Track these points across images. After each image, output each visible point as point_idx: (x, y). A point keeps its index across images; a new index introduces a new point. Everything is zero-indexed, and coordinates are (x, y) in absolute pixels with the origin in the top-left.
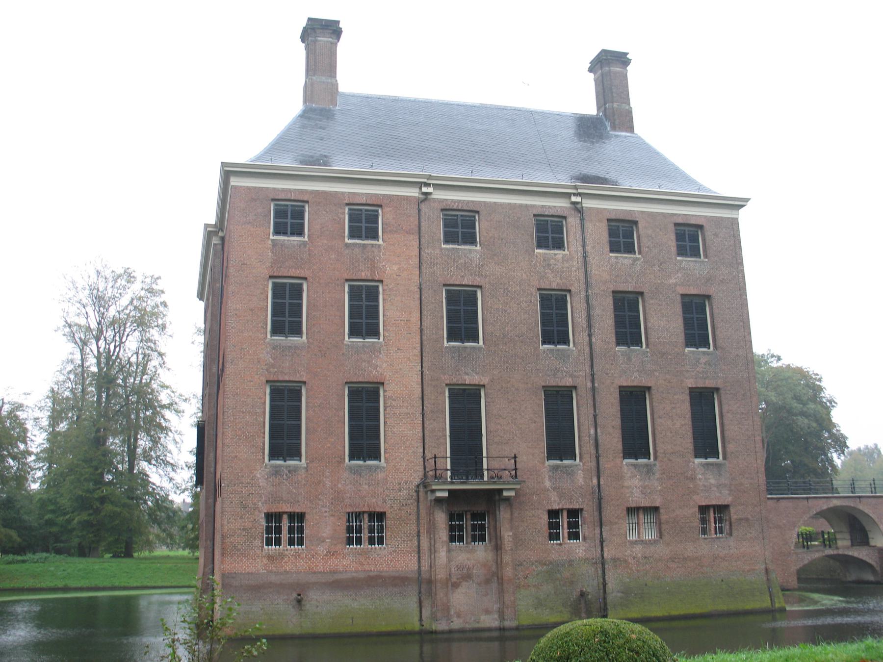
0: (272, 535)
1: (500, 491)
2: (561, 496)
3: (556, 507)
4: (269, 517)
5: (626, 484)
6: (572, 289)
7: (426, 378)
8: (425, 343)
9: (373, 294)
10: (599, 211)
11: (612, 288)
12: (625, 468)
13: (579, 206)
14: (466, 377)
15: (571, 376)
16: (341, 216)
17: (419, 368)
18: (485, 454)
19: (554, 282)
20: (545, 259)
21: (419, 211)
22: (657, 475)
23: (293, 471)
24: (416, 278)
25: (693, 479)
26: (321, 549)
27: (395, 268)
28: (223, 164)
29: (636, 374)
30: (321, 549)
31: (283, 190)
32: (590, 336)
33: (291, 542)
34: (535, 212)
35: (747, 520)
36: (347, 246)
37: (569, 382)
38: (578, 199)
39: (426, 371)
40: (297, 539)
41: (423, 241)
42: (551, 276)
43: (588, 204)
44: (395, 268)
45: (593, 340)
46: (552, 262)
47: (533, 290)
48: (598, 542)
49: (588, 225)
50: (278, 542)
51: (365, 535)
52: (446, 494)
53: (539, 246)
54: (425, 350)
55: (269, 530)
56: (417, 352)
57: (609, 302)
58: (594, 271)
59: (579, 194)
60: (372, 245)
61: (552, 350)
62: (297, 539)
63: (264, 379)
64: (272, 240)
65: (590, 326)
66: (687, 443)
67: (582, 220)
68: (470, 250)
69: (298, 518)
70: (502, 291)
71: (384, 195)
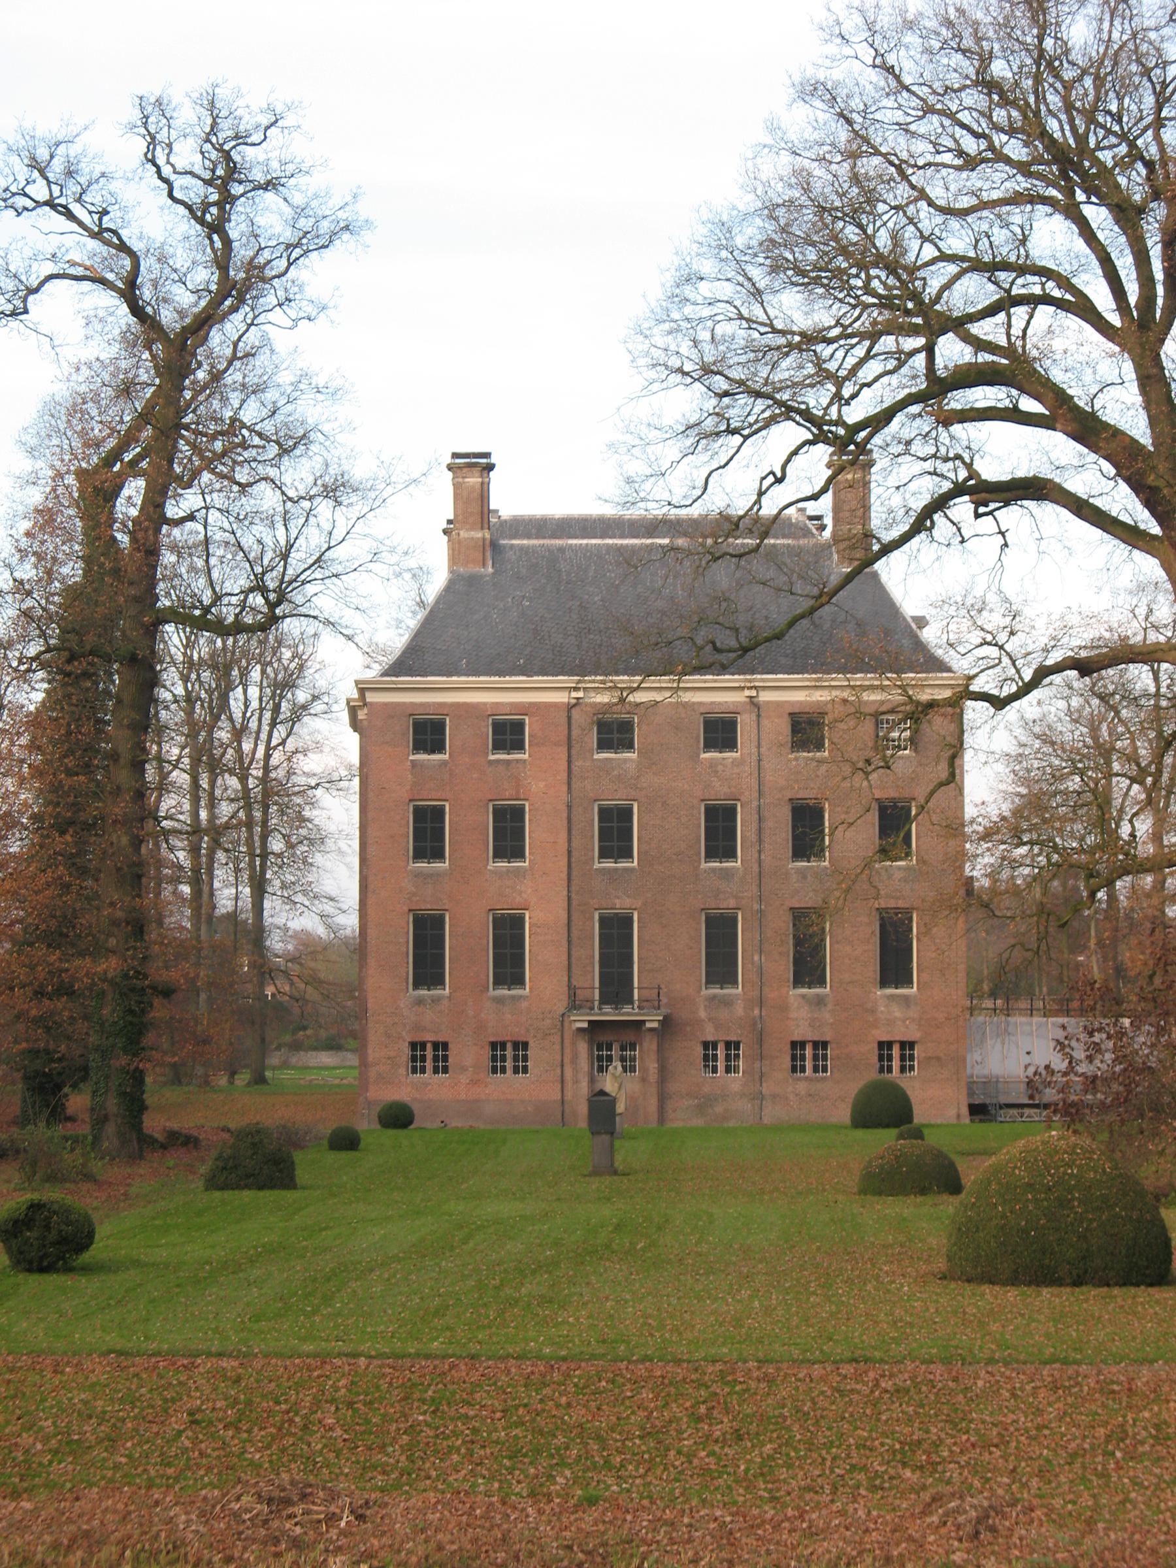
0: (417, 1063)
1: (644, 1022)
2: (717, 1028)
3: (710, 1038)
4: (413, 1046)
5: (791, 1016)
6: (742, 798)
7: (574, 903)
8: (573, 865)
9: (517, 814)
10: (779, 705)
11: (789, 795)
12: (792, 1000)
13: (755, 700)
14: (617, 901)
15: (736, 897)
16: (484, 730)
17: (565, 893)
18: (636, 984)
19: (719, 791)
20: (712, 764)
21: (569, 718)
22: (830, 1007)
23: (436, 1000)
24: (564, 796)
25: (873, 1011)
26: (464, 1079)
27: (541, 785)
28: (357, 682)
29: (811, 894)
30: (464, 1079)
31: (422, 705)
32: (760, 852)
33: (436, 1070)
34: (702, 710)
35: (938, 1059)
36: (491, 762)
37: (732, 903)
38: (753, 693)
39: (573, 896)
40: (442, 1065)
41: (573, 752)
42: (717, 784)
43: (765, 697)
44: (541, 785)
45: (763, 857)
46: (720, 768)
47: (695, 802)
48: (757, 1077)
49: (765, 722)
50: (423, 1071)
51: (509, 1064)
52: (585, 1025)
53: (709, 745)
54: (574, 873)
55: (414, 1059)
56: (564, 875)
57: (786, 814)
58: (768, 777)
59: (755, 687)
60: (517, 761)
61: (713, 870)
62: (442, 1065)
63: (406, 909)
64: (412, 761)
65: (760, 841)
66: (873, 969)
67: (759, 716)
68: (625, 760)
69: (441, 1046)
70: (659, 805)
71: (530, 704)
